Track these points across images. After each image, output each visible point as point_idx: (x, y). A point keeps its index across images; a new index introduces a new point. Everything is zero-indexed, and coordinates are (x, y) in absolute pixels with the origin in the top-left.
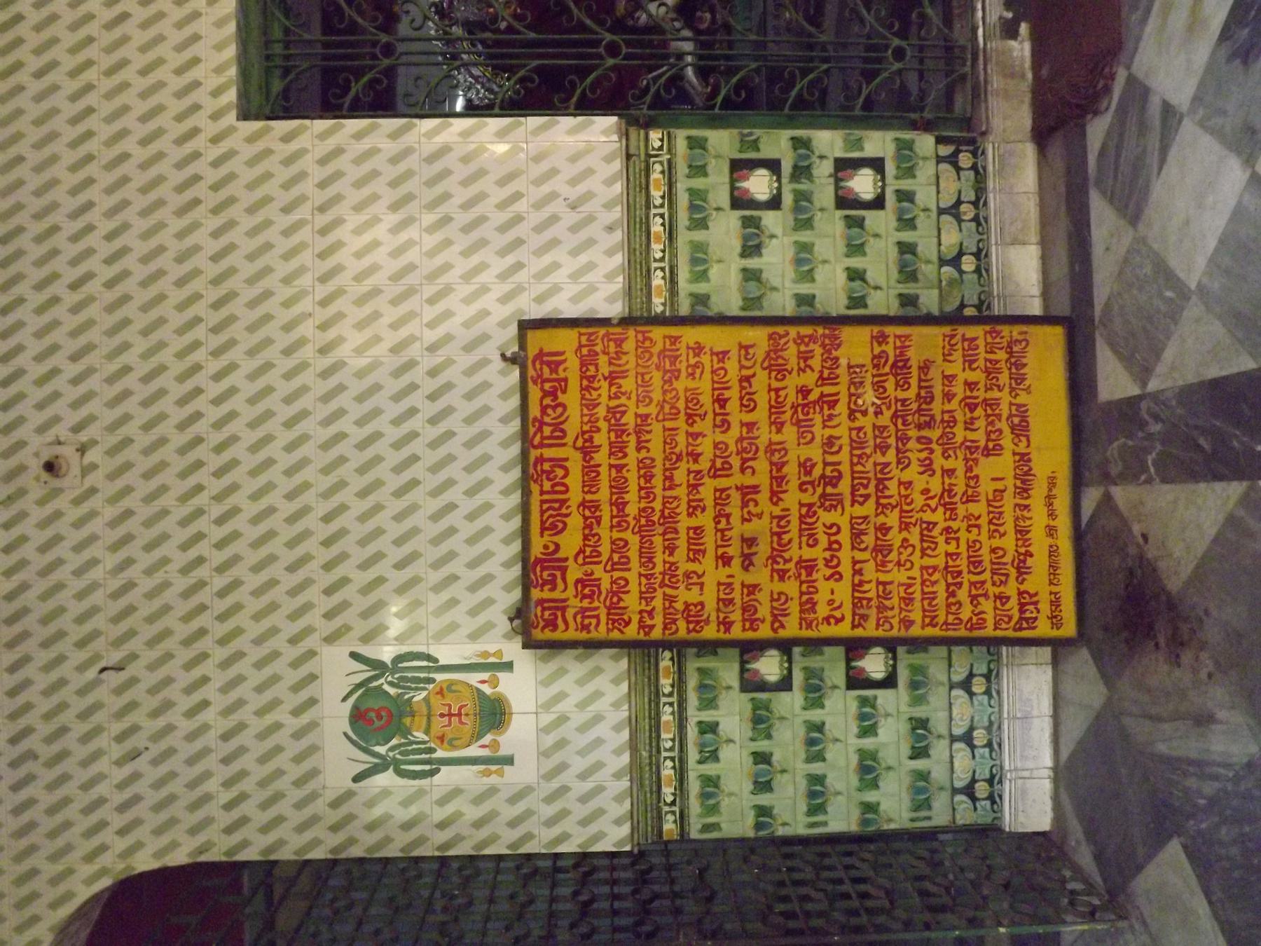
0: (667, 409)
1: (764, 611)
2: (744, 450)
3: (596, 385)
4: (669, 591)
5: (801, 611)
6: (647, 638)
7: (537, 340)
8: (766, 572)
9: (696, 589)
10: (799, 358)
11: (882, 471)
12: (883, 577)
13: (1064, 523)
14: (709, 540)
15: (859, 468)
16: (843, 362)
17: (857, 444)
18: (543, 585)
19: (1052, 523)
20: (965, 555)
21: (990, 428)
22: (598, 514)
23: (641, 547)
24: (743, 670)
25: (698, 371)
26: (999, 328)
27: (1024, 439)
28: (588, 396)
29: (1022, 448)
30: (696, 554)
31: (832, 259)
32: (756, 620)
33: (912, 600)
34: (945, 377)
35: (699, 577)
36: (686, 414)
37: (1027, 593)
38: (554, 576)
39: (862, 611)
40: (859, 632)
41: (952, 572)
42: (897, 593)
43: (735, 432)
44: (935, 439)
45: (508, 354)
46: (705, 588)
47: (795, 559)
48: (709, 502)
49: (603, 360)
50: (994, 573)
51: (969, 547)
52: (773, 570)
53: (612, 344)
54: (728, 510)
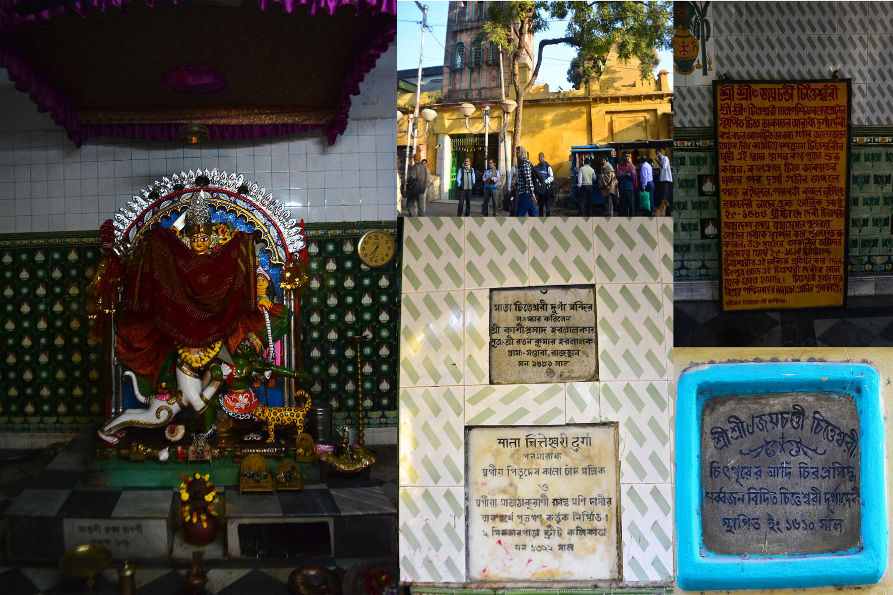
1: (731, 186)
8: (746, 187)
12: (745, 234)
16: (831, 218)
17: (798, 224)
24: (707, 176)
29: (796, 289)
30: (754, 157)
40: (723, 225)
42: (739, 240)
43: (803, 173)
48: (775, 163)
49: (834, 116)
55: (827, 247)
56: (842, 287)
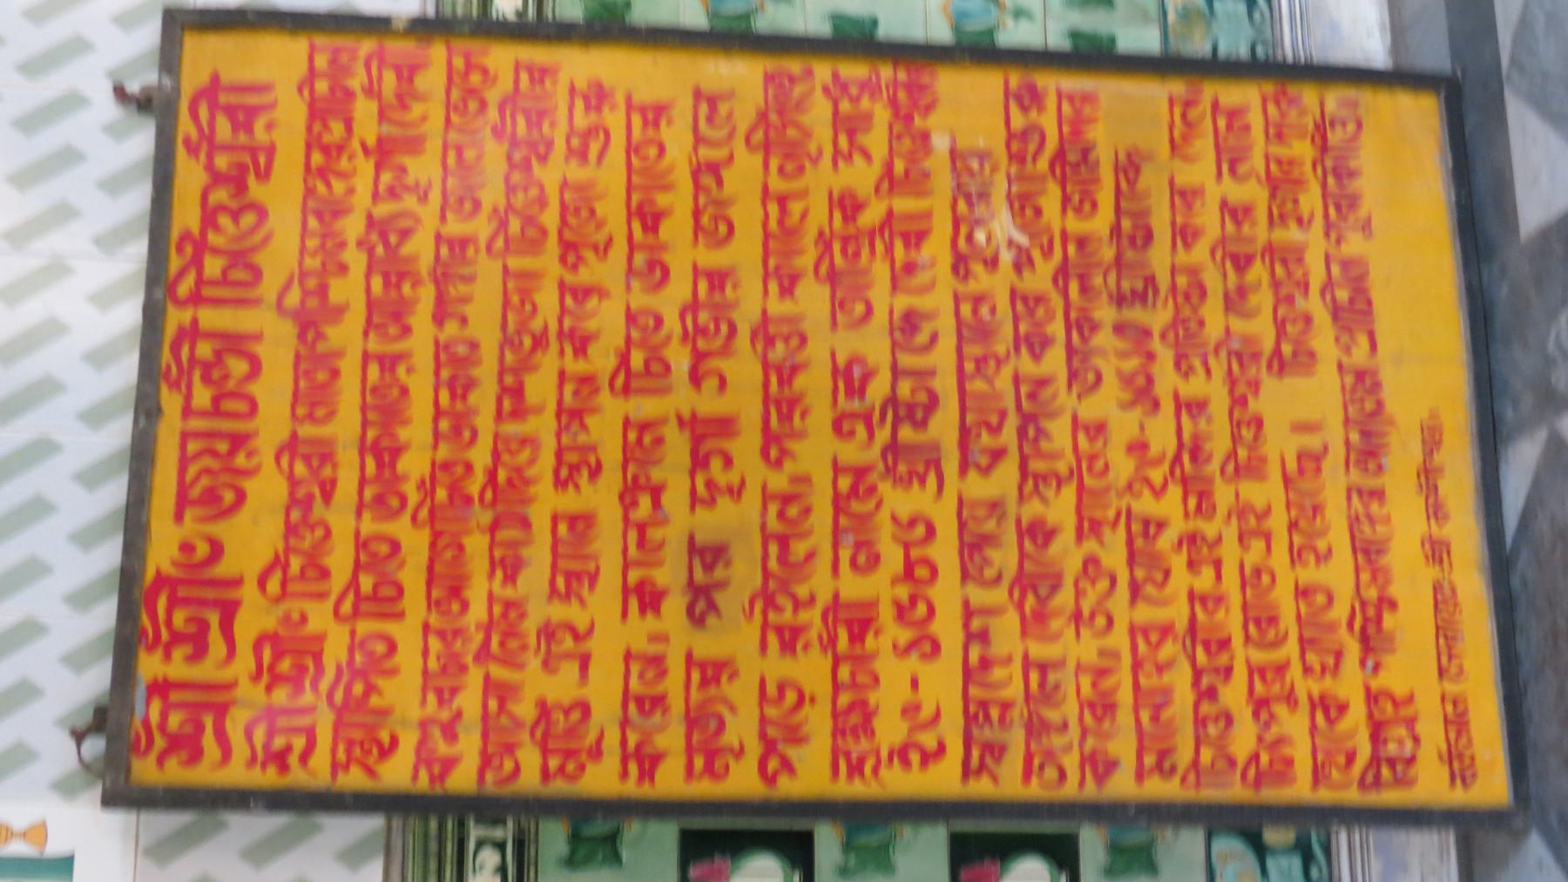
0: (515, 226)
1: (742, 728)
3: (344, 164)
4: (498, 672)
5: (838, 732)
6: (438, 790)
7: (205, 56)
9: (570, 670)
11: (1032, 396)
12: (1038, 650)
13: (1464, 531)
14: (608, 545)
16: (940, 143)
17: (974, 331)
20: (1235, 599)
22: (327, 471)
26: (1293, 89)
28: (321, 188)
30: (573, 579)
38: (204, 627)
40: (981, 788)
43: (679, 289)
45: (134, 87)
46: (593, 669)
47: (824, 598)
48: (611, 454)
49: (365, 110)
52: (765, 626)
54: (656, 475)
56: (1334, 98)
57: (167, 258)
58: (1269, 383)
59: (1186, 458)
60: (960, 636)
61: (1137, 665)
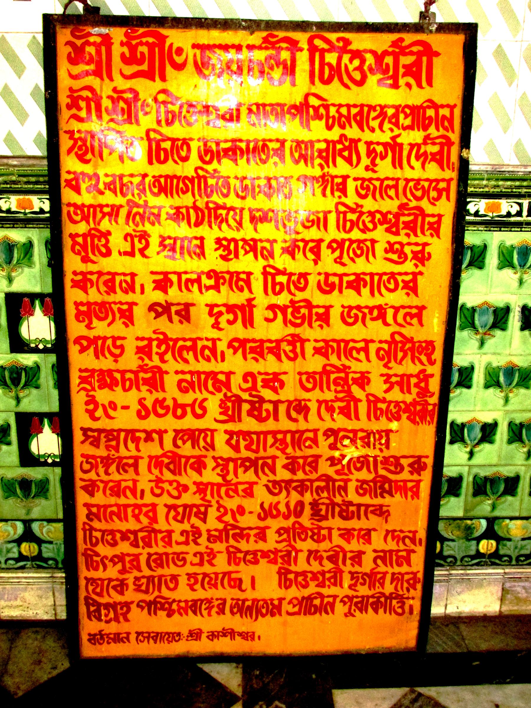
0: (350, 216)
1: (100, 328)
2: (297, 310)
4: (123, 212)
5: (101, 371)
6: (63, 184)
7: (451, 47)
8: (148, 334)
10: (402, 376)
11: (265, 464)
12: (143, 465)
15: (270, 440)
16: (394, 425)
18: (127, 44)
19: (204, 636)
20: (169, 550)
21: (310, 575)
23: (178, 178)
25: (395, 257)
26: (419, 586)
27: (296, 609)
29: (286, 607)
31: (509, 407)
32: (91, 322)
33: (119, 497)
34: (369, 532)
35: (142, 252)
36: (343, 241)
37: (129, 610)
38: (140, 62)
39: (103, 440)
41: (149, 537)
43: (319, 299)
44: (299, 520)
46: (128, 257)
48: (234, 266)
49: (417, 136)
50: (150, 579)
51: (178, 554)
52: (150, 340)
53: (435, 149)
54: (224, 289)
55: (378, 501)
57: (335, 31)
58: (275, 568)
59: (238, 531)
60: (149, 429)
61: (136, 506)
